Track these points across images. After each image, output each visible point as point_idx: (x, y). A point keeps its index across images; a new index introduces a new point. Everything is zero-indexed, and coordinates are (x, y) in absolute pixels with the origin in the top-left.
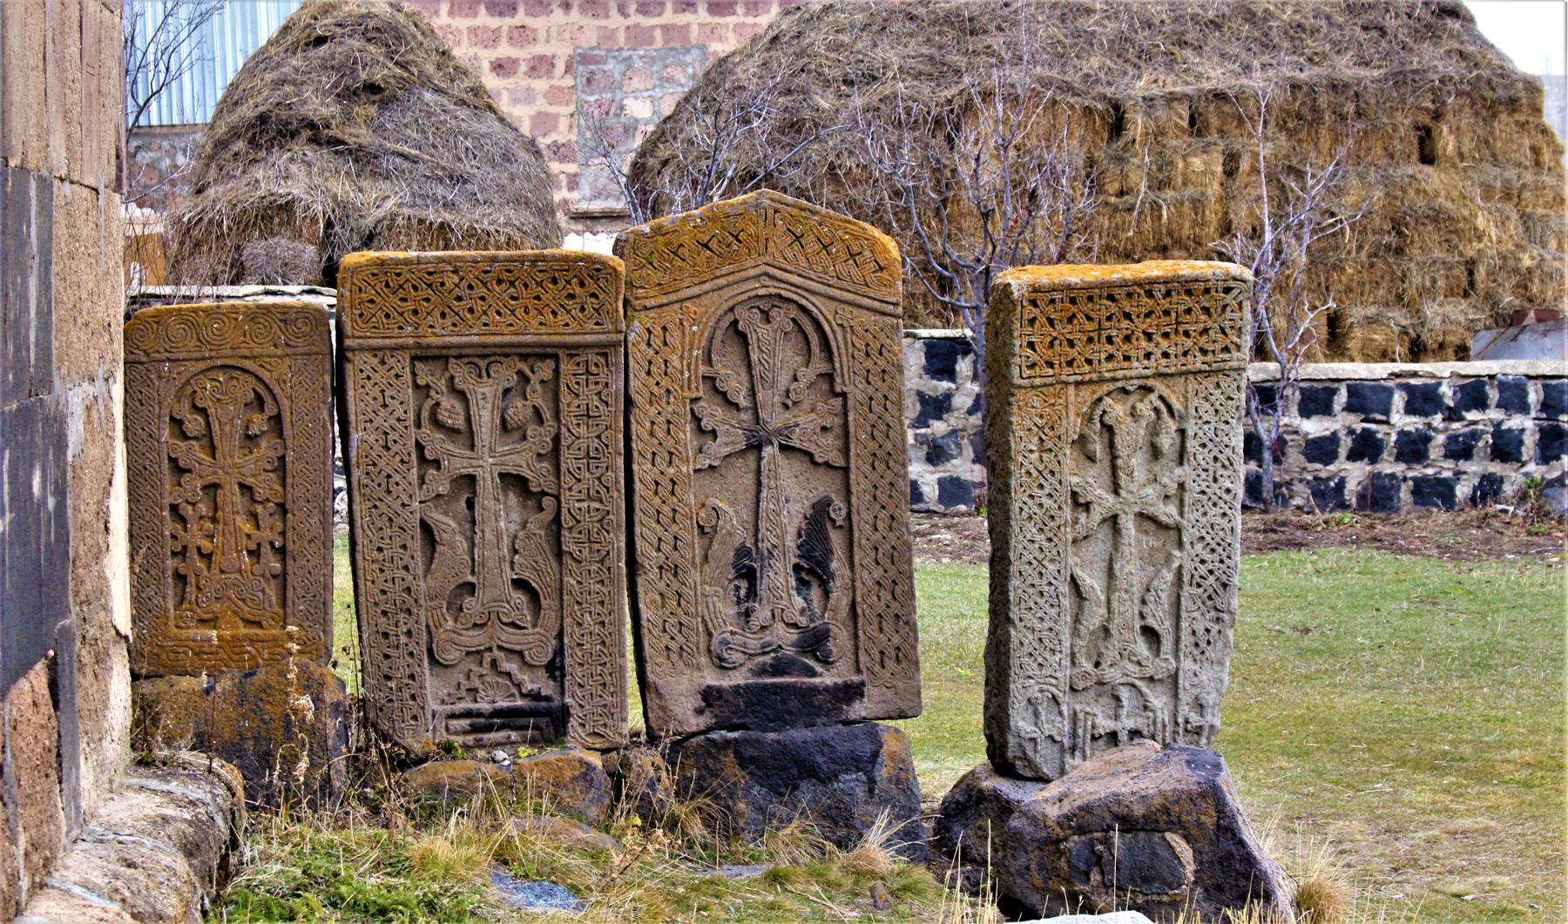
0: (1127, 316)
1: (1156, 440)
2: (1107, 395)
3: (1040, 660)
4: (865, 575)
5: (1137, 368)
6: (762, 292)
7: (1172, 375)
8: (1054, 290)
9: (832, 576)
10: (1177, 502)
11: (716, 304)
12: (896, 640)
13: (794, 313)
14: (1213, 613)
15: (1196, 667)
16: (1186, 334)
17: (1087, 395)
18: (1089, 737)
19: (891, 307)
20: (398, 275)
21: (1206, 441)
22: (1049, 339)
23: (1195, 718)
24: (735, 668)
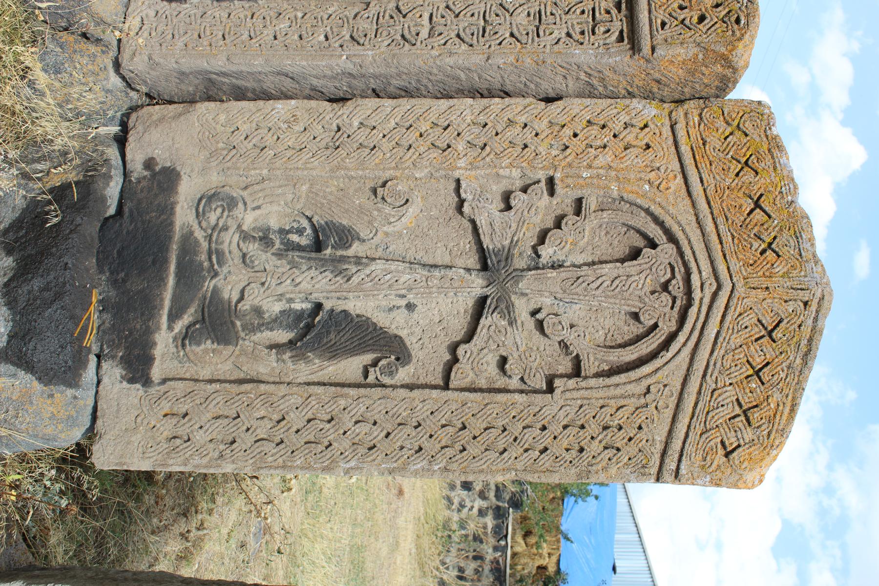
12: (200, 437)
13: (667, 327)
19: (673, 466)
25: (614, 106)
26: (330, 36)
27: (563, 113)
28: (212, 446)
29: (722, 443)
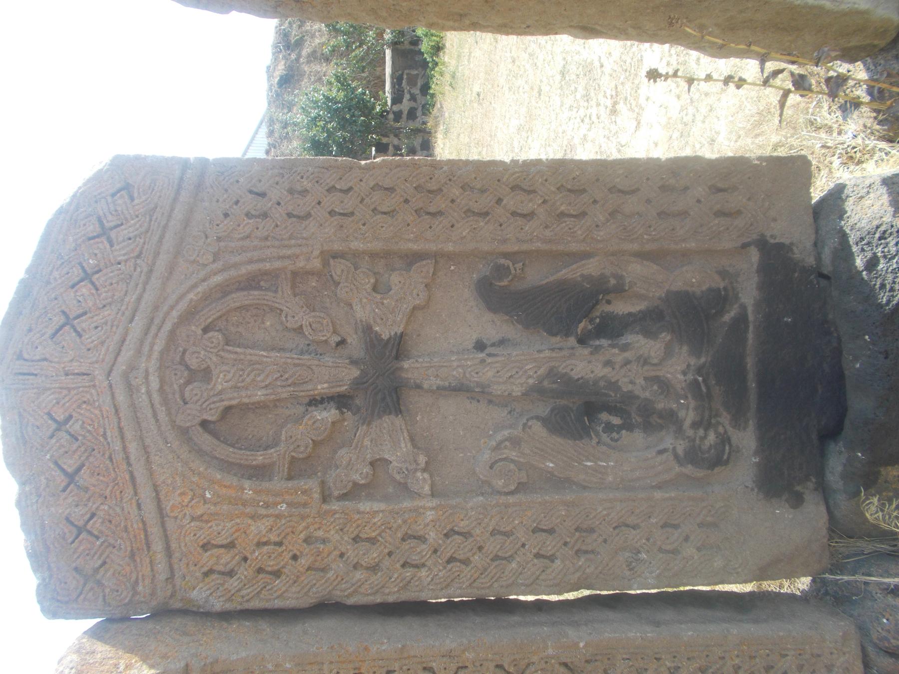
25: (245, 599)
27: (308, 587)
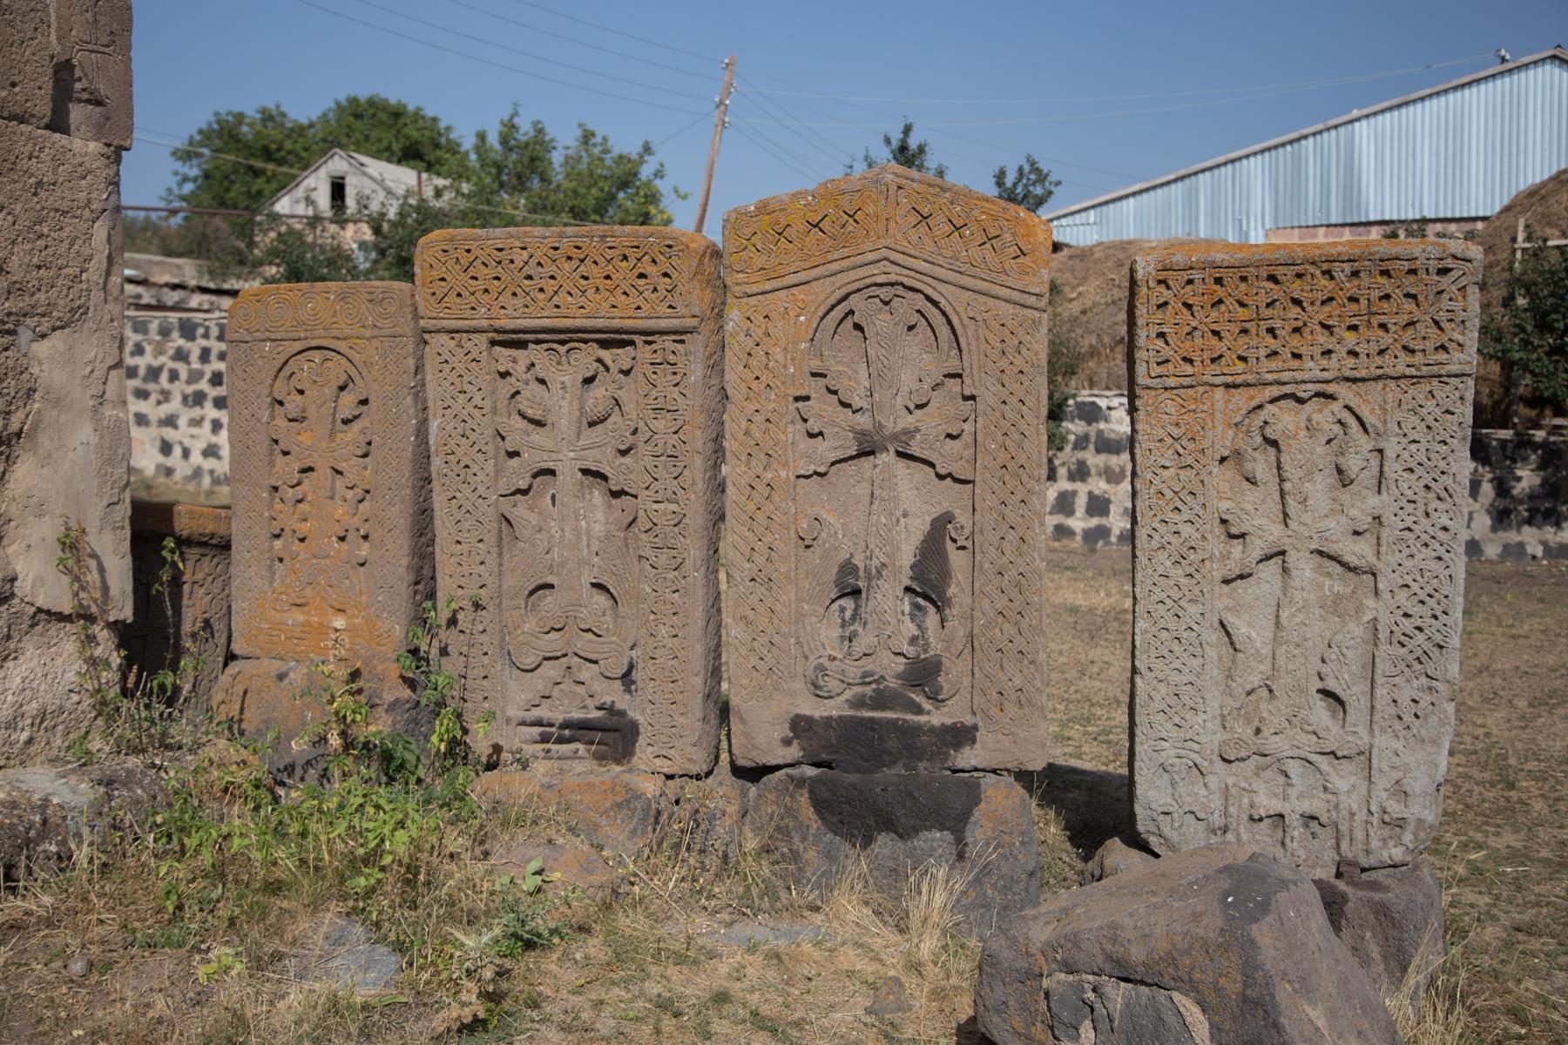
0: (1297, 302)
1: (1341, 460)
2: (1271, 402)
3: (1177, 720)
4: (986, 604)
5: (1311, 370)
6: (881, 279)
7: (1363, 380)
8: (1191, 268)
9: (948, 602)
10: (1374, 541)
11: (825, 291)
12: (1018, 682)
14: (1424, 680)
15: (1398, 745)
16: (1383, 326)
17: (1242, 399)
18: (1245, 817)
19: (1033, 298)
20: (468, 251)
21: (1413, 465)
22: (1188, 329)
23: (1395, 808)
24: (831, 697)
26: (675, 588)
28: (1025, 670)
29: (1014, 258)
